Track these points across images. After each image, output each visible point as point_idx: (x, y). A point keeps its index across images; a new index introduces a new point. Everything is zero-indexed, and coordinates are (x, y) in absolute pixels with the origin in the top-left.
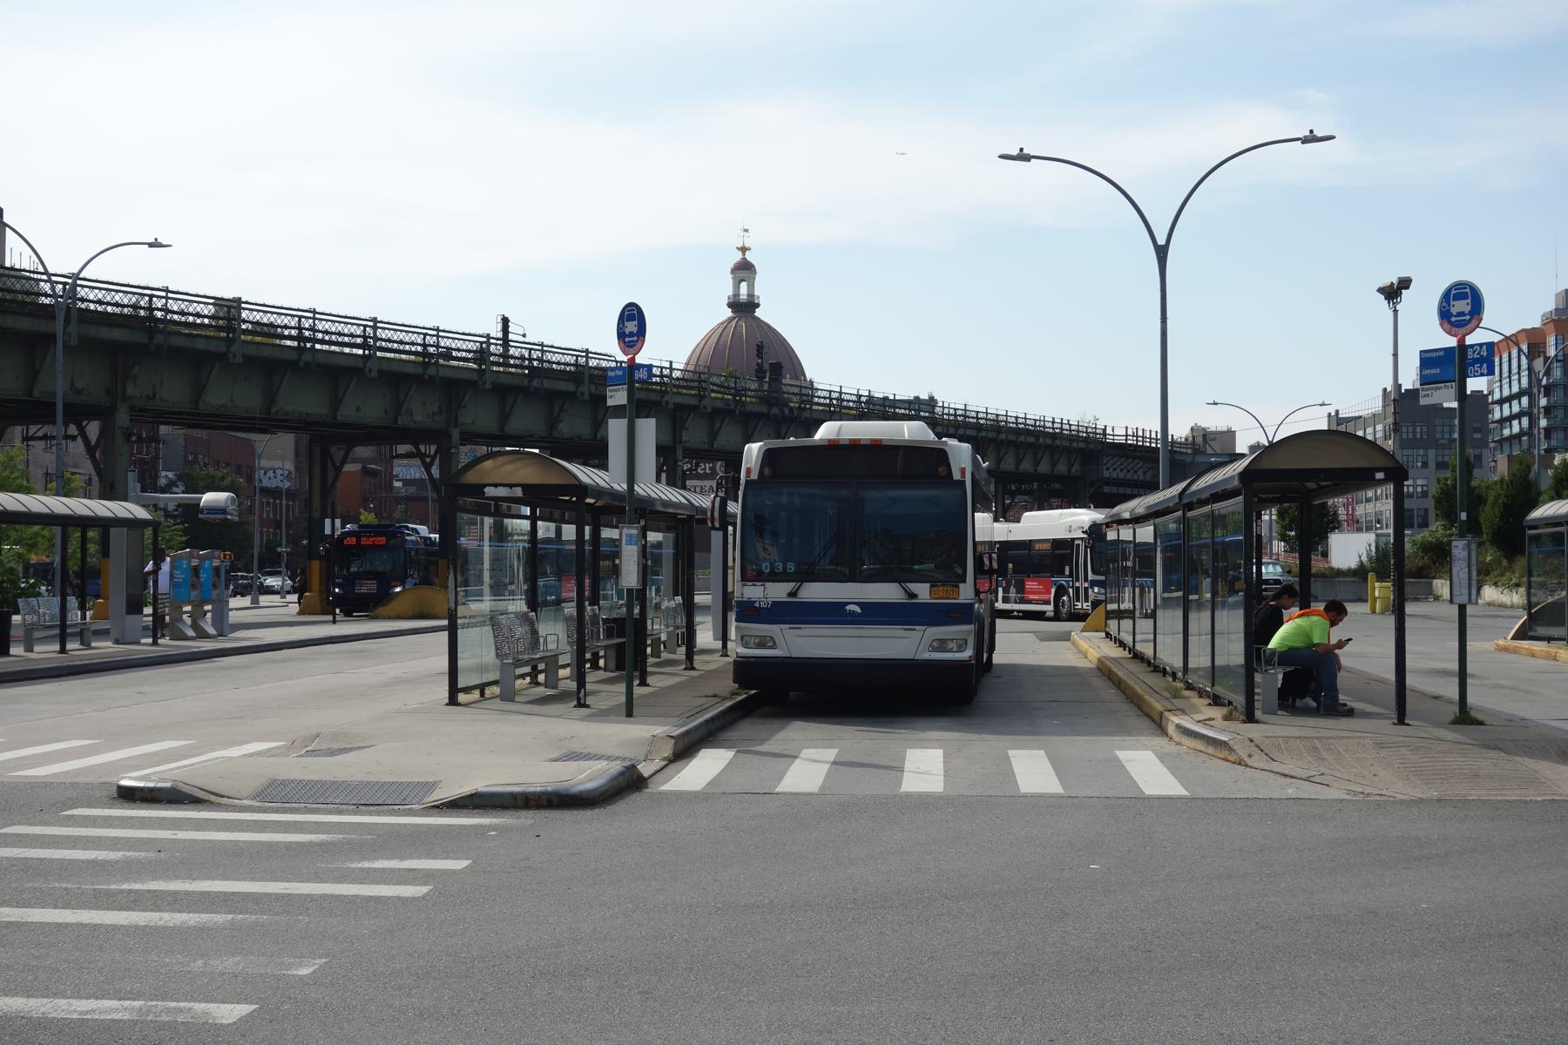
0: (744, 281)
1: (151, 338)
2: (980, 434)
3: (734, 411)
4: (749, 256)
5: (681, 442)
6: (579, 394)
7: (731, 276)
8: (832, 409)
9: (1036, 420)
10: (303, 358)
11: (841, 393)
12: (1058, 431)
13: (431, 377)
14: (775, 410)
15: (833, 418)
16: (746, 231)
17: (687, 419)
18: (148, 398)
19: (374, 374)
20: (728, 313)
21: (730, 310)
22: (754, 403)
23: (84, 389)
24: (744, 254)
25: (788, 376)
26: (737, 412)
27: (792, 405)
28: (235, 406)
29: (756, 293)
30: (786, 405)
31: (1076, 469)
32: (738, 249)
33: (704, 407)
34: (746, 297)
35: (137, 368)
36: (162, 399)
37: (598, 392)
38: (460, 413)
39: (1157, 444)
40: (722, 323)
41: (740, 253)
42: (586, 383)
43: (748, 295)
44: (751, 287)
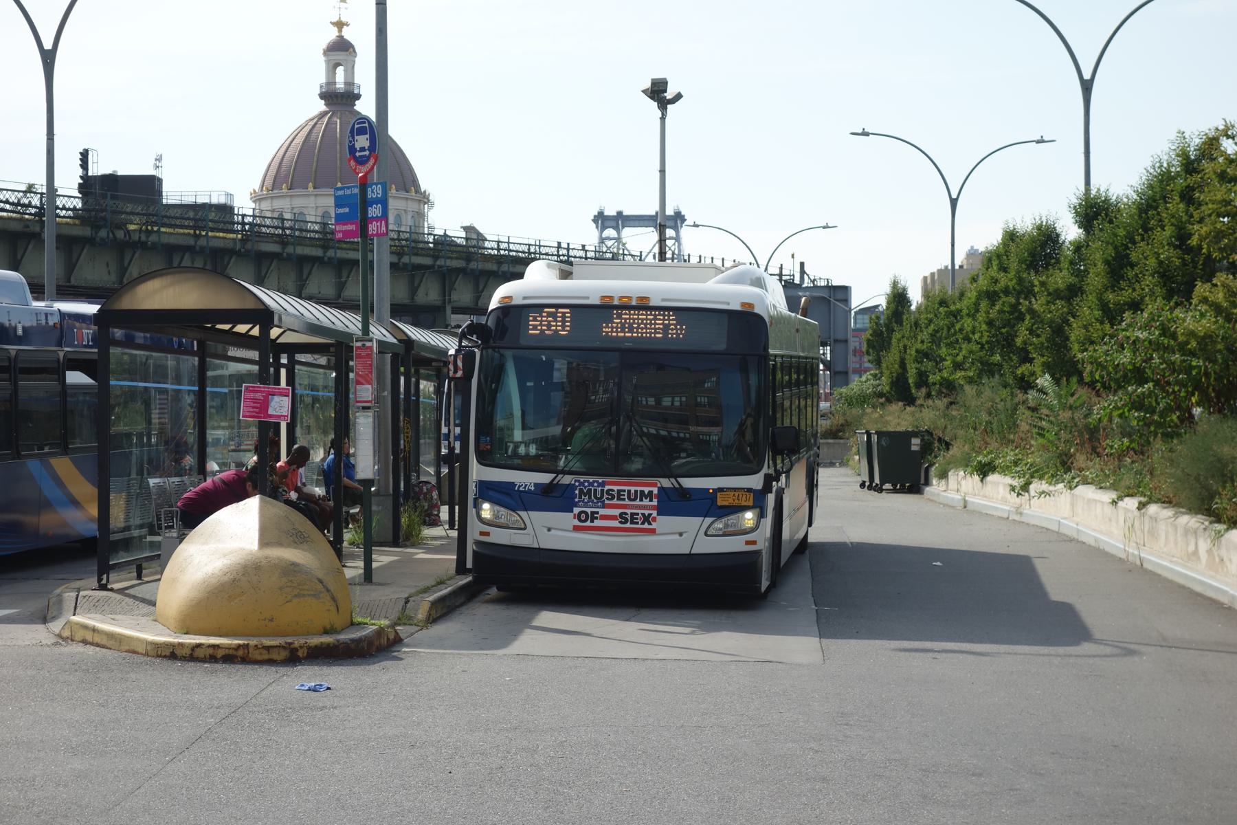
0: (338, 64)
2: (438, 263)
4: (347, 34)
7: (323, 59)
8: (198, 232)
9: (529, 245)
14: (103, 233)
20: (321, 106)
21: (323, 102)
22: (75, 225)
24: (340, 30)
25: (394, 186)
27: (132, 227)
29: (357, 80)
30: (122, 226)
32: (333, 24)
34: (343, 86)
40: (311, 120)
41: (336, 29)
43: (346, 83)
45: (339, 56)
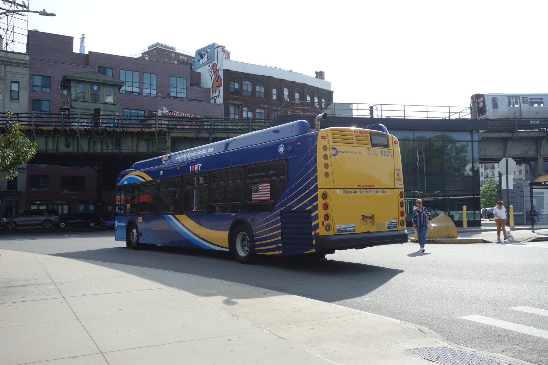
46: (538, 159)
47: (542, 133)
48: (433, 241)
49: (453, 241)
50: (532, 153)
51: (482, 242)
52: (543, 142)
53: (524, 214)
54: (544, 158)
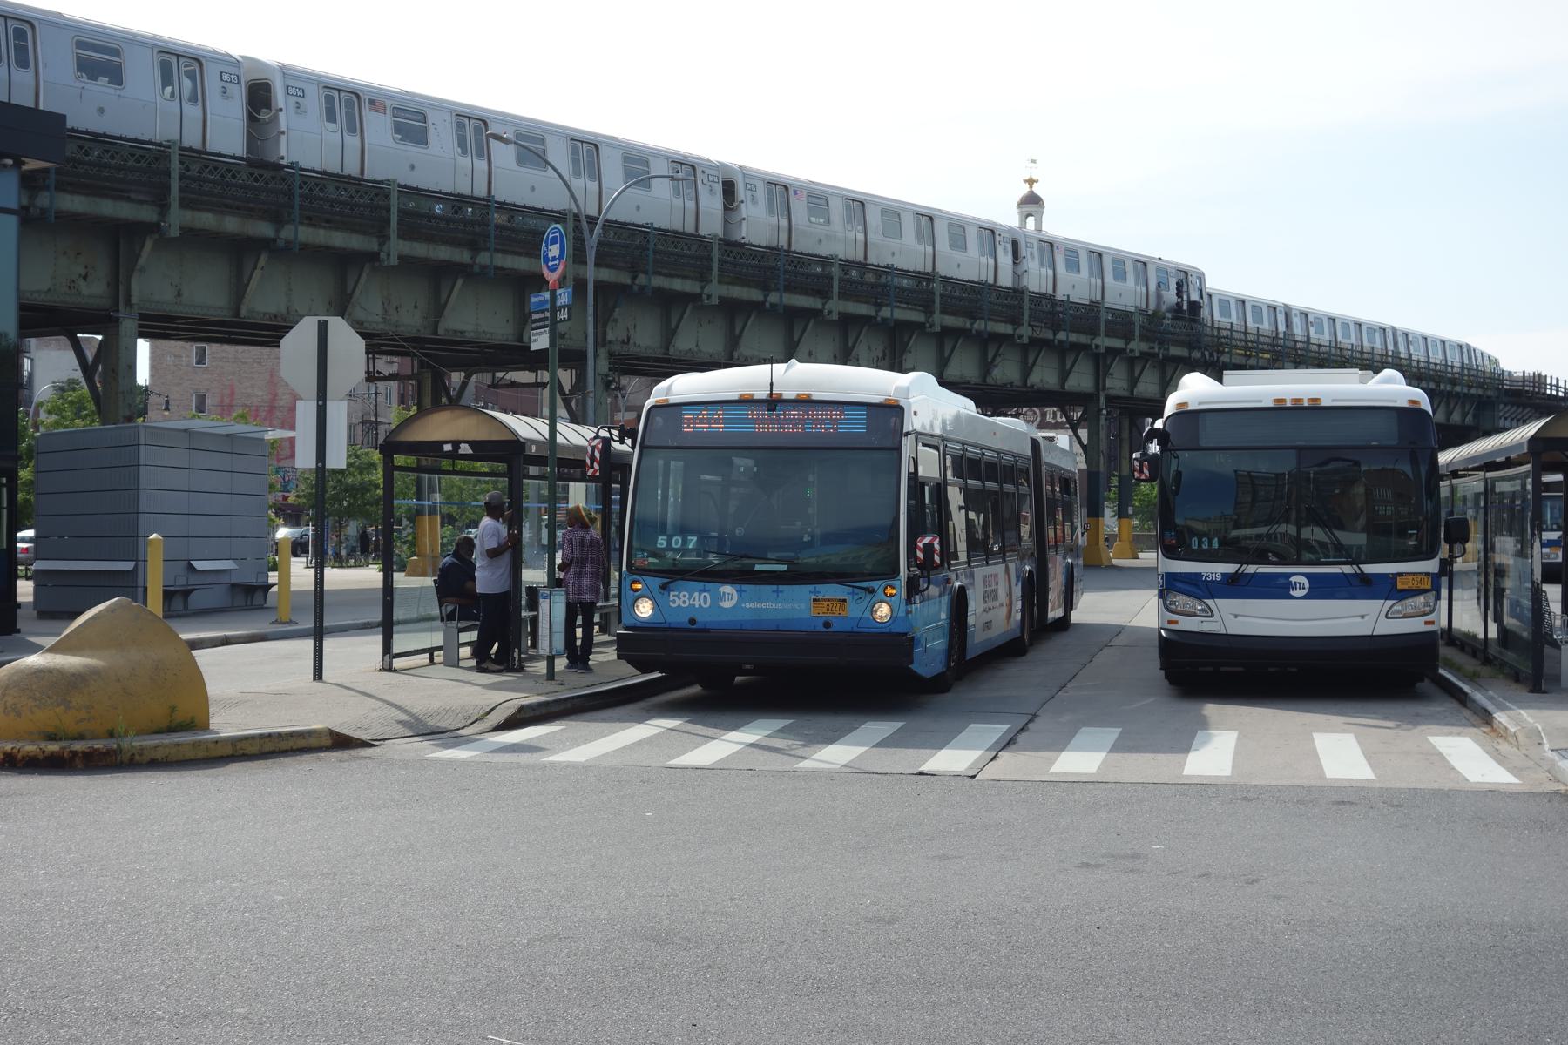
0: (1032, 215)
1: (634, 278)
3: (1158, 354)
4: (1037, 189)
5: (1104, 388)
6: (1016, 337)
8: (1248, 353)
10: (768, 299)
11: (1258, 335)
12: (1457, 376)
13: (884, 320)
14: (1197, 354)
15: (1276, 365)
16: (1034, 161)
17: (1111, 365)
18: (623, 342)
19: (835, 317)
23: (566, 334)
24: (1031, 187)
26: (1161, 356)
28: (700, 351)
29: (1043, 229)
31: (1469, 420)
32: (1025, 181)
33: (1132, 351)
35: (617, 310)
36: (635, 343)
37: (1035, 335)
38: (904, 357)
39: (1557, 391)
41: (1027, 185)
42: (1026, 324)
44: (1039, 223)
45: (1029, 208)
46: (117, 320)
47: (145, 206)
48: (108, 753)
49: (208, 749)
50: (94, 291)
51: (329, 742)
52: (142, 247)
53: (136, 566)
54: (143, 317)
